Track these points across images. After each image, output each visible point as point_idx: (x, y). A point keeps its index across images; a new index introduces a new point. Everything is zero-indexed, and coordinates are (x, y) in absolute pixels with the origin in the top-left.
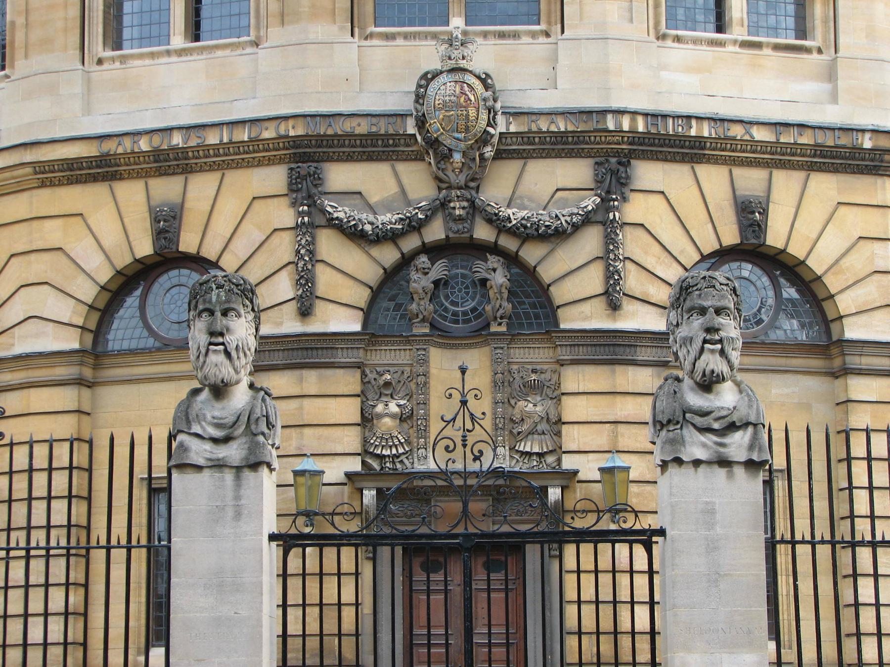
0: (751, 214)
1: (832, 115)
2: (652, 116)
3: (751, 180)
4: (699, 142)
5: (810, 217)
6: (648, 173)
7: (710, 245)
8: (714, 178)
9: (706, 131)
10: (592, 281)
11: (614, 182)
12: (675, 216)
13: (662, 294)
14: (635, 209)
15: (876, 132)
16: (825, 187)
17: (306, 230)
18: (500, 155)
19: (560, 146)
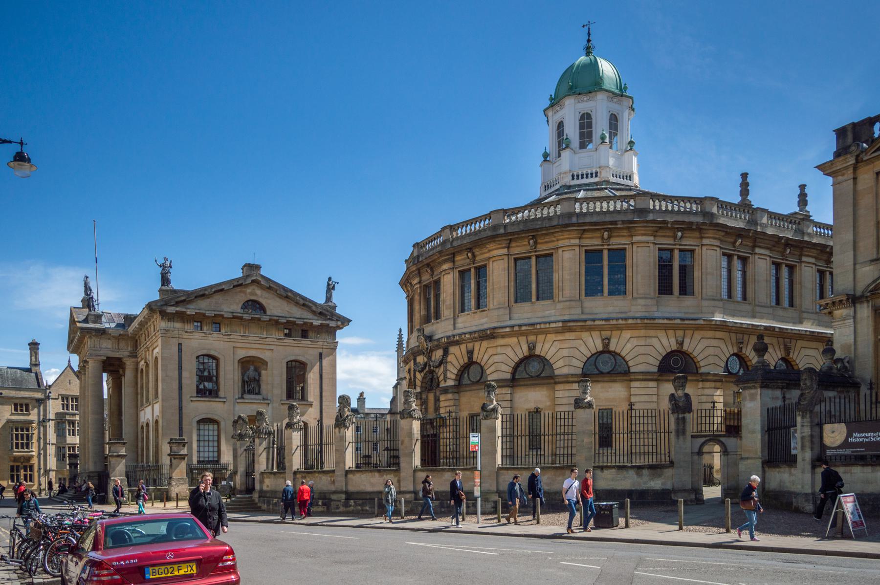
0: (470, 353)
1: (486, 326)
2: (448, 337)
3: (470, 346)
4: (457, 341)
5: (483, 352)
6: (452, 349)
7: (462, 363)
8: (463, 347)
9: (457, 338)
10: (442, 378)
11: (446, 353)
12: (457, 357)
13: (454, 377)
14: (450, 358)
15: (490, 329)
16: (485, 344)
17: (415, 371)
18: (432, 351)
19: (438, 347)
